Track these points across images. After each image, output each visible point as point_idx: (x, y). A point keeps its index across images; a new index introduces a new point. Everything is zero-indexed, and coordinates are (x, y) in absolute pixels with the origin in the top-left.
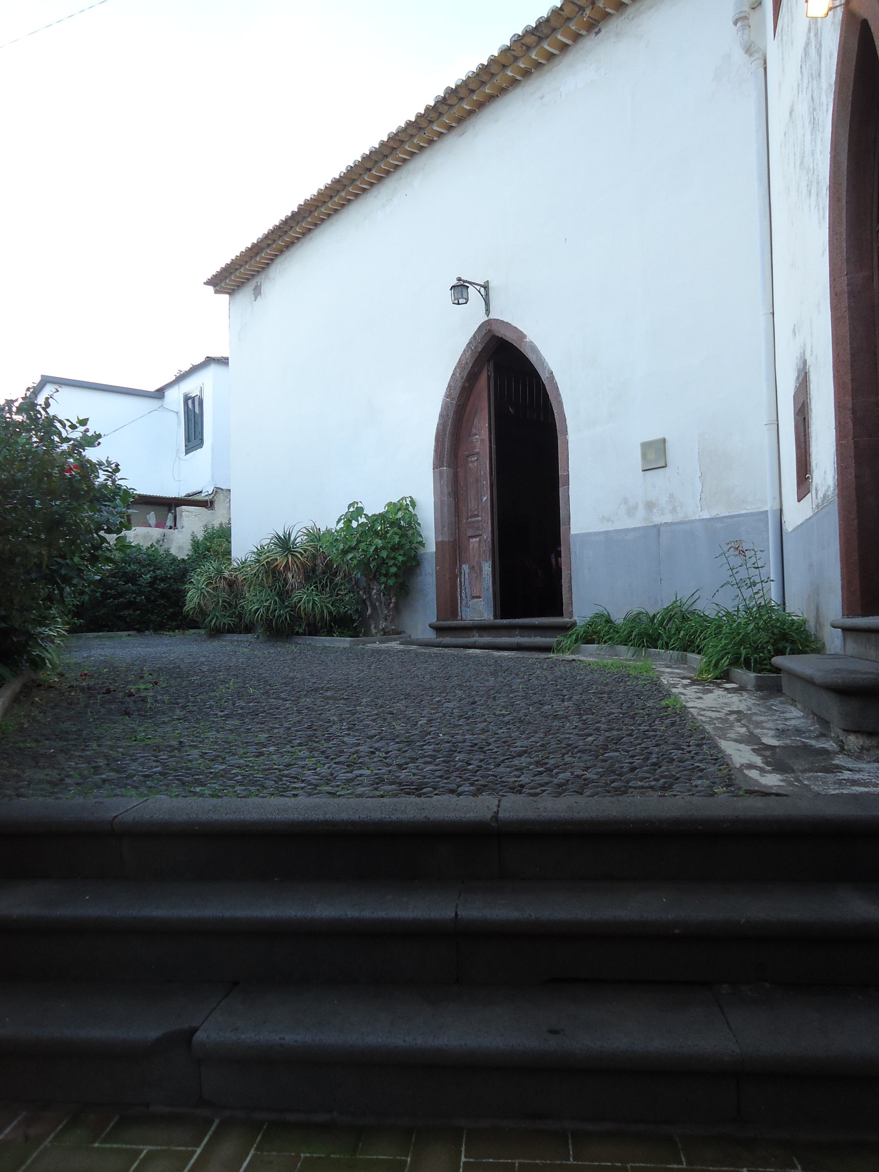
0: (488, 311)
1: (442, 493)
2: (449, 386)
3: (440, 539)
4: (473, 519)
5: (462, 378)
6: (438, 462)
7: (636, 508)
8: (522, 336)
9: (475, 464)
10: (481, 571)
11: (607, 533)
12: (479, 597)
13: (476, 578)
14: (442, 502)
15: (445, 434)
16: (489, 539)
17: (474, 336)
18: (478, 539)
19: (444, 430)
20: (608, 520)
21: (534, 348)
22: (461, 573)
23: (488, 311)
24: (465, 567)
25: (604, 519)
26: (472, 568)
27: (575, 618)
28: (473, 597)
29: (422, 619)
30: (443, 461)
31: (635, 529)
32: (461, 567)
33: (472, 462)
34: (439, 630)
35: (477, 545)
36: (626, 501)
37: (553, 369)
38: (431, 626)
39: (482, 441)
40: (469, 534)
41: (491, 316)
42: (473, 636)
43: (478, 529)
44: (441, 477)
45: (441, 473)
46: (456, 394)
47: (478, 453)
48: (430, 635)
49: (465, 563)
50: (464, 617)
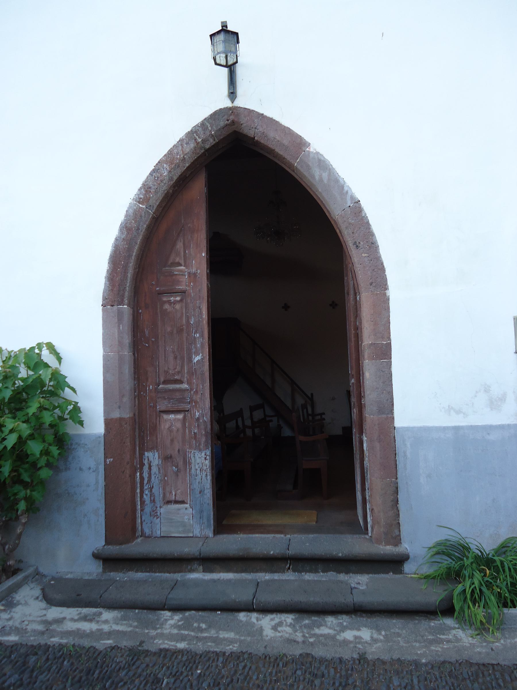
0: (232, 94)
1: (120, 343)
2: (146, 187)
3: (116, 414)
4: (171, 387)
5: (171, 179)
6: (112, 297)
7: (503, 399)
8: (299, 143)
9: (178, 306)
10: (187, 462)
11: (457, 429)
12: (183, 502)
13: (177, 474)
14: (121, 359)
15: (130, 256)
16: (207, 418)
17: (203, 124)
18: (180, 416)
19: (129, 250)
20: (458, 412)
21: (323, 164)
22: (142, 465)
23: (232, 94)
24: (153, 458)
25: (450, 409)
26: (167, 458)
27: (406, 547)
28: (169, 502)
29: (72, 542)
30: (123, 296)
31: (502, 427)
32: (142, 455)
33: (169, 302)
34: (109, 562)
35: (179, 425)
36: (487, 389)
37: (359, 196)
38: (96, 556)
39: (193, 276)
40: (162, 405)
41: (240, 102)
42: (191, 571)
43: (182, 400)
44: (120, 320)
45: (120, 314)
46: (156, 200)
47: (184, 292)
48: (93, 569)
49: (151, 449)
50: (147, 531)
